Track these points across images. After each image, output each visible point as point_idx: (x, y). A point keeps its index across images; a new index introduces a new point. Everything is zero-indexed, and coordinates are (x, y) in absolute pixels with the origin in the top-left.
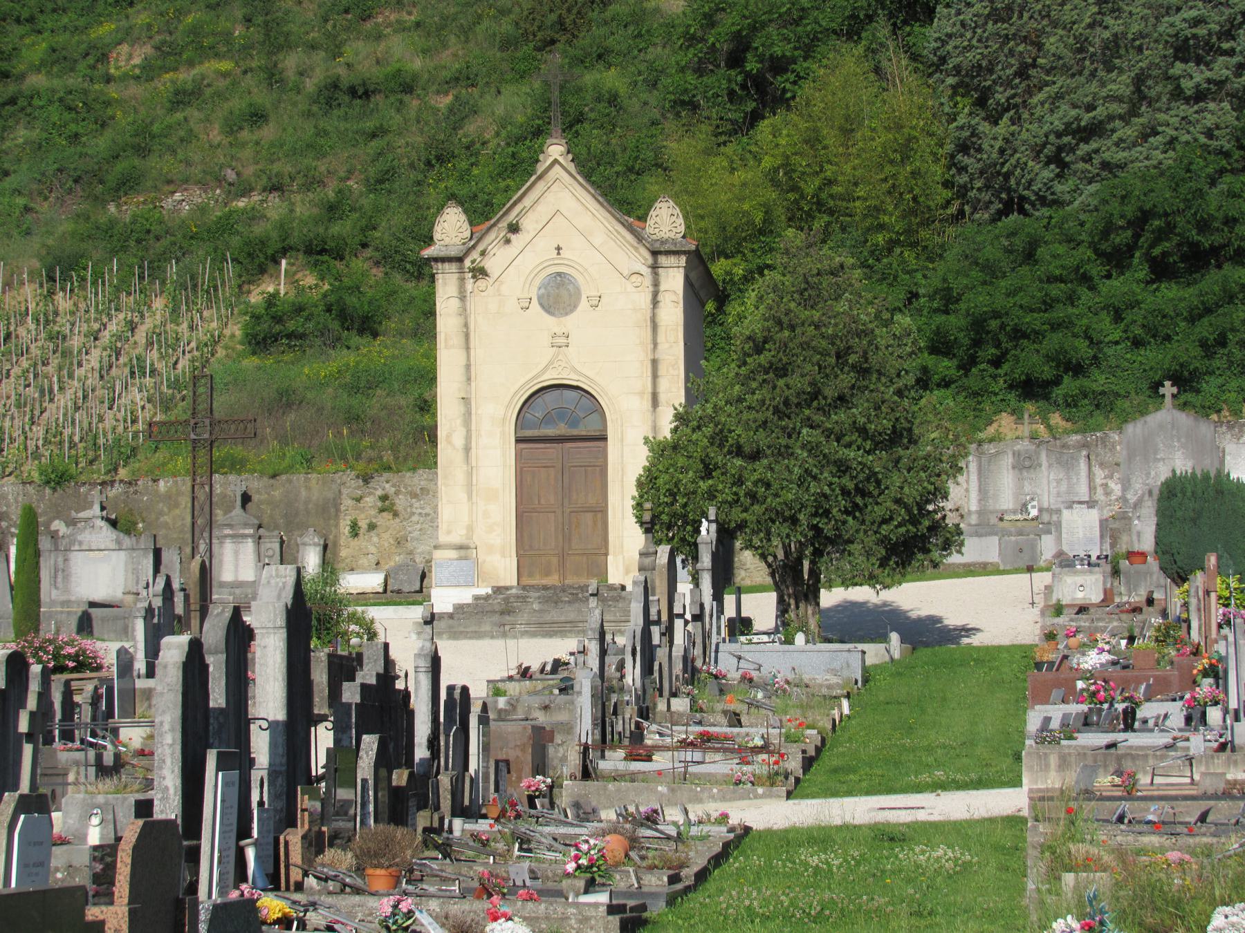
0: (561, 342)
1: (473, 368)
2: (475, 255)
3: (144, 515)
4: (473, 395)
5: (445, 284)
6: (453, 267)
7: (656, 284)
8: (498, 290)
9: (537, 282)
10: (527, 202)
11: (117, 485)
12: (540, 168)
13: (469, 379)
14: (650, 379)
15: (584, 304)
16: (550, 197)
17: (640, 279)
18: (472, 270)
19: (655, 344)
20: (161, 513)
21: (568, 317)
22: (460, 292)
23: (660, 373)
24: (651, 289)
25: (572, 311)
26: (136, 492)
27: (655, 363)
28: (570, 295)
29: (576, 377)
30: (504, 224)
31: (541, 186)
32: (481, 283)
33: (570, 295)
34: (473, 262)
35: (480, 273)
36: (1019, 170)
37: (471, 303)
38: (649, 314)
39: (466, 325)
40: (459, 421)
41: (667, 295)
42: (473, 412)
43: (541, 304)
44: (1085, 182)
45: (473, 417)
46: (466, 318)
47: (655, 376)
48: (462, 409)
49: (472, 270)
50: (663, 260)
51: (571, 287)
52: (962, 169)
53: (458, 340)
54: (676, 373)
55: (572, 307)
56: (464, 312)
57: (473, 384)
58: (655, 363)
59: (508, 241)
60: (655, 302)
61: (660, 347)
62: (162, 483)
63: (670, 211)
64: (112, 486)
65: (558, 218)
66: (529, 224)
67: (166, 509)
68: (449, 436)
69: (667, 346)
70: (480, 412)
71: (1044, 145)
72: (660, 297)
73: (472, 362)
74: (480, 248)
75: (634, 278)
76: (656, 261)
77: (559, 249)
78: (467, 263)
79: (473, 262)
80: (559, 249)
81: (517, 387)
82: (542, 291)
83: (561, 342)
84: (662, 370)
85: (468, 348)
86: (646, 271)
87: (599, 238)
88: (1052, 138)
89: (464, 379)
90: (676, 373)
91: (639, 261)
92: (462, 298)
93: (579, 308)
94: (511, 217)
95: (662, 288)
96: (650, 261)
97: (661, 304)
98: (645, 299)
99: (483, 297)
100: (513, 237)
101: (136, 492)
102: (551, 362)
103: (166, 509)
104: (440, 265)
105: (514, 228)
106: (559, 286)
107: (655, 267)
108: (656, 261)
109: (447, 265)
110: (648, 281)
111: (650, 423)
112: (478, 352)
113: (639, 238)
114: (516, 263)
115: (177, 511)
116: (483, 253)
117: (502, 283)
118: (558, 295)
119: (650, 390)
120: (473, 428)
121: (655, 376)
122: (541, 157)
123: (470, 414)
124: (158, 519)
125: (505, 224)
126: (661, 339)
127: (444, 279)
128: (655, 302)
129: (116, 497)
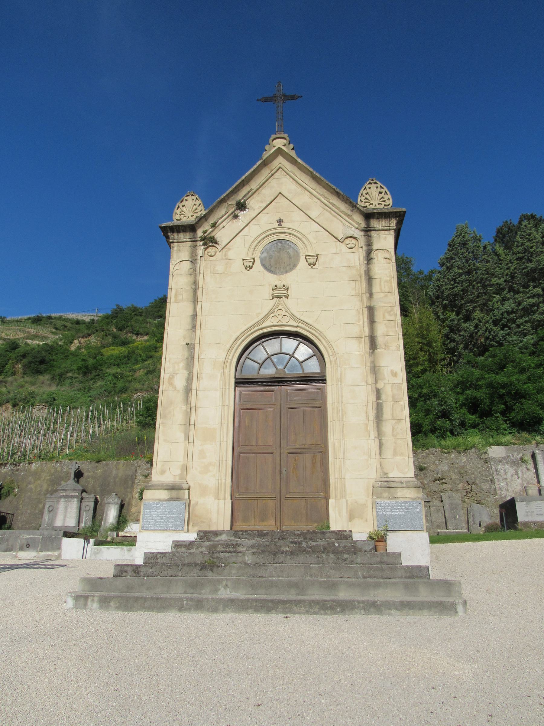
0: (280, 294)
1: (198, 318)
2: (206, 226)
3: (19, 483)
4: (197, 341)
5: (179, 250)
6: (187, 236)
7: (369, 244)
8: (226, 255)
9: (261, 247)
10: (253, 185)
11: (8, 466)
12: (265, 155)
13: (194, 327)
14: (366, 325)
15: (302, 263)
16: (273, 182)
17: (354, 241)
18: (203, 239)
19: (371, 294)
20: (30, 483)
21: (288, 274)
22: (192, 256)
23: (376, 319)
24: (365, 248)
25: (291, 269)
26: (18, 470)
27: (371, 310)
28: (290, 257)
29: (295, 324)
30: (232, 202)
31: (265, 173)
32: (211, 250)
33: (290, 257)
34: (205, 232)
35: (210, 241)
36: (487, 333)
37: (200, 266)
38: (363, 269)
39: (195, 283)
40: (182, 365)
41: (380, 253)
42: (196, 355)
43: (263, 265)
44: (522, 336)
45: (196, 361)
46: (195, 277)
47: (372, 321)
48: (186, 354)
49: (203, 239)
50: (375, 223)
51: (290, 251)
52: (454, 341)
53: (186, 295)
54: (392, 318)
55: (293, 266)
56: (194, 272)
57: (198, 332)
58: (371, 310)
59: (236, 217)
60: (369, 259)
61: (375, 296)
62: (34, 465)
63: (379, 190)
64: (5, 466)
65: (280, 199)
66: (255, 204)
67: (33, 481)
68: (171, 378)
69: (382, 295)
70: (202, 357)
71: (501, 319)
72: (373, 255)
73: (199, 313)
74: (211, 220)
75: (348, 241)
76: (368, 225)
77: (280, 221)
78: (200, 233)
79: (205, 232)
80: (280, 221)
81: (238, 334)
82: (265, 254)
83: (280, 294)
84: (379, 315)
85: (195, 301)
86: (359, 234)
87: (316, 210)
88: (506, 315)
89: (189, 327)
90: (392, 318)
91: (353, 225)
92: (193, 261)
93: (298, 267)
94: (240, 196)
95: (375, 247)
96: (363, 225)
97: (374, 261)
98: (357, 257)
99: (212, 264)
100: (241, 214)
101: (18, 470)
102: (271, 312)
103: (33, 481)
104: (175, 235)
105: (241, 206)
106: (279, 250)
107: (367, 230)
108: (368, 225)
109: (181, 235)
110: (362, 242)
111: (369, 364)
112: (204, 306)
113: (353, 206)
114: (240, 235)
115: (39, 482)
116: (214, 225)
117: (229, 249)
118: (279, 256)
119: (367, 333)
120: (195, 370)
121: (372, 321)
122: (267, 147)
123: (193, 358)
124: (27, 486)
125: (234, 203)
126: (376, 289)
127: (178, 246)
128: (369, 259)
129: (6, 473)
